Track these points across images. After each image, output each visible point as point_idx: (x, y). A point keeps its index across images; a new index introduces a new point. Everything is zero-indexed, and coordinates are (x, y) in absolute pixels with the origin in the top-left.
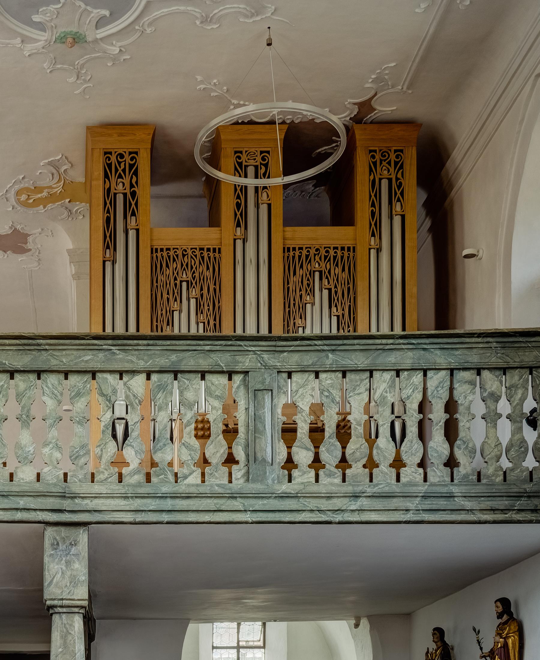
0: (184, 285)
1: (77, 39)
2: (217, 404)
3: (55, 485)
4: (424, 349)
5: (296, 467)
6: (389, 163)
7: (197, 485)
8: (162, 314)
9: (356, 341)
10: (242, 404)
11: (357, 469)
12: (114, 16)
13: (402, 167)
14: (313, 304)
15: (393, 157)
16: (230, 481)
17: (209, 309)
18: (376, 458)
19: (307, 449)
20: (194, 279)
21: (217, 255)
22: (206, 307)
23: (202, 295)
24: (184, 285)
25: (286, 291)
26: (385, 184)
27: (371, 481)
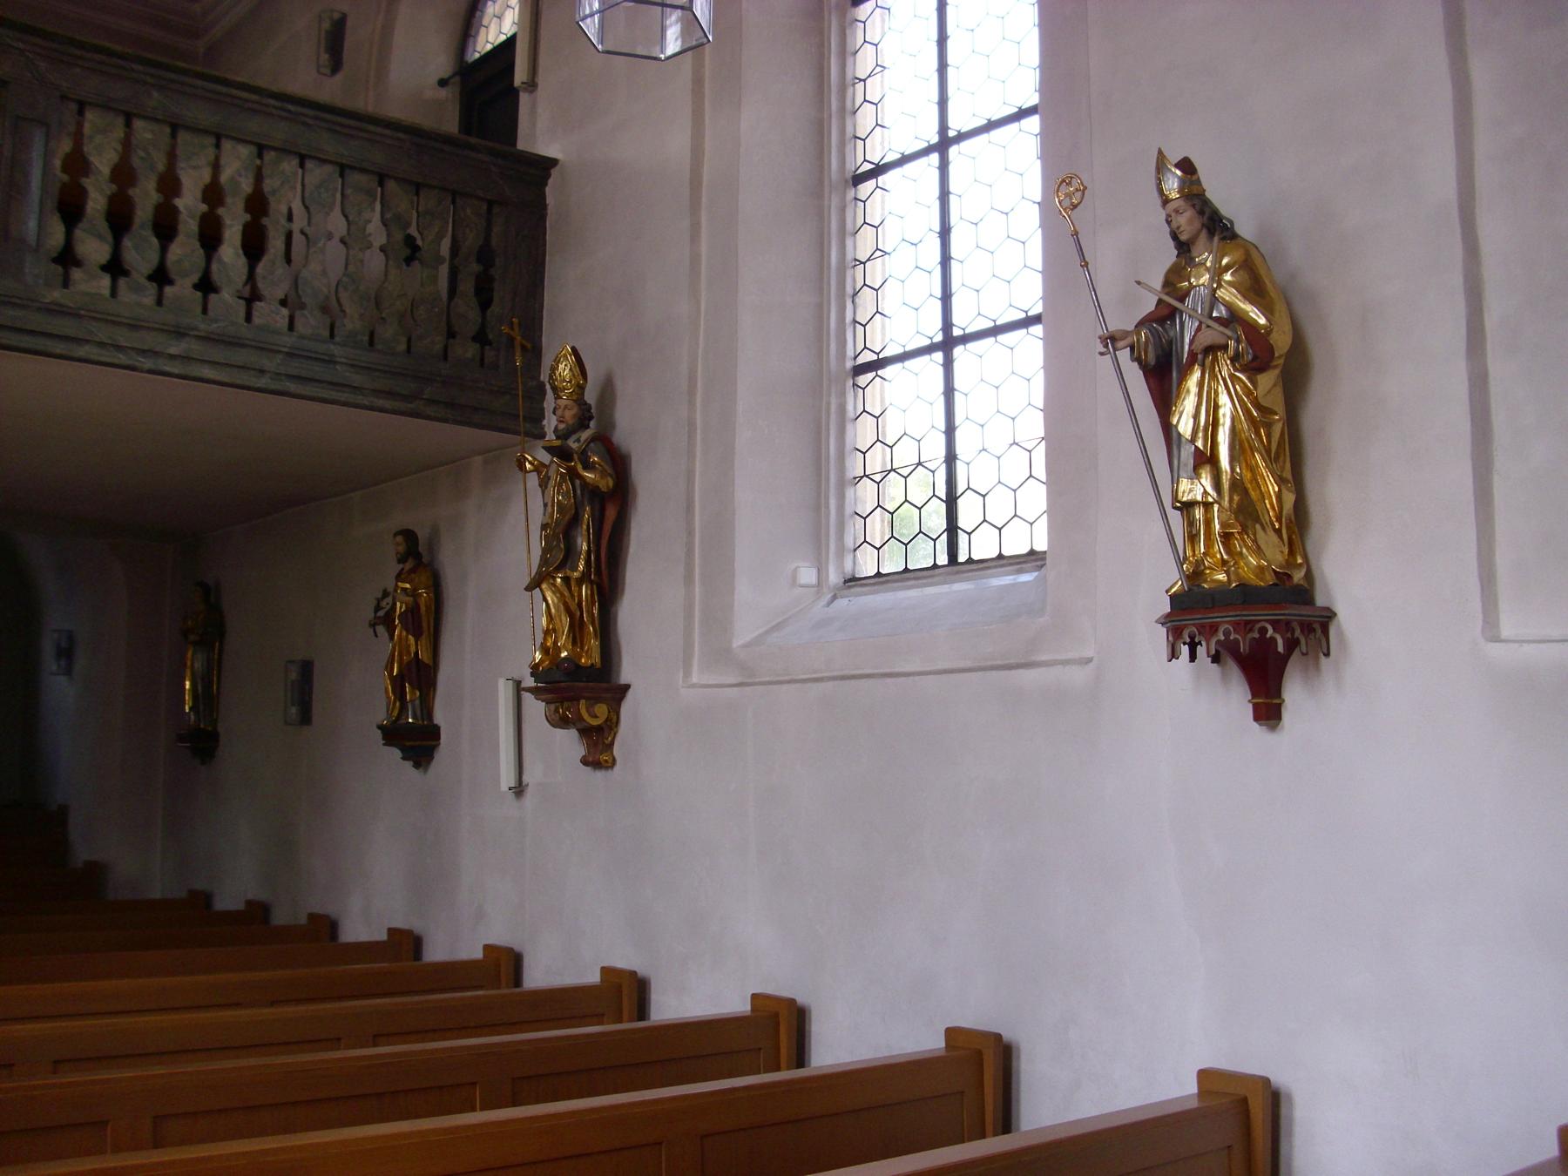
4: (304, 124)
5: (78, 263)
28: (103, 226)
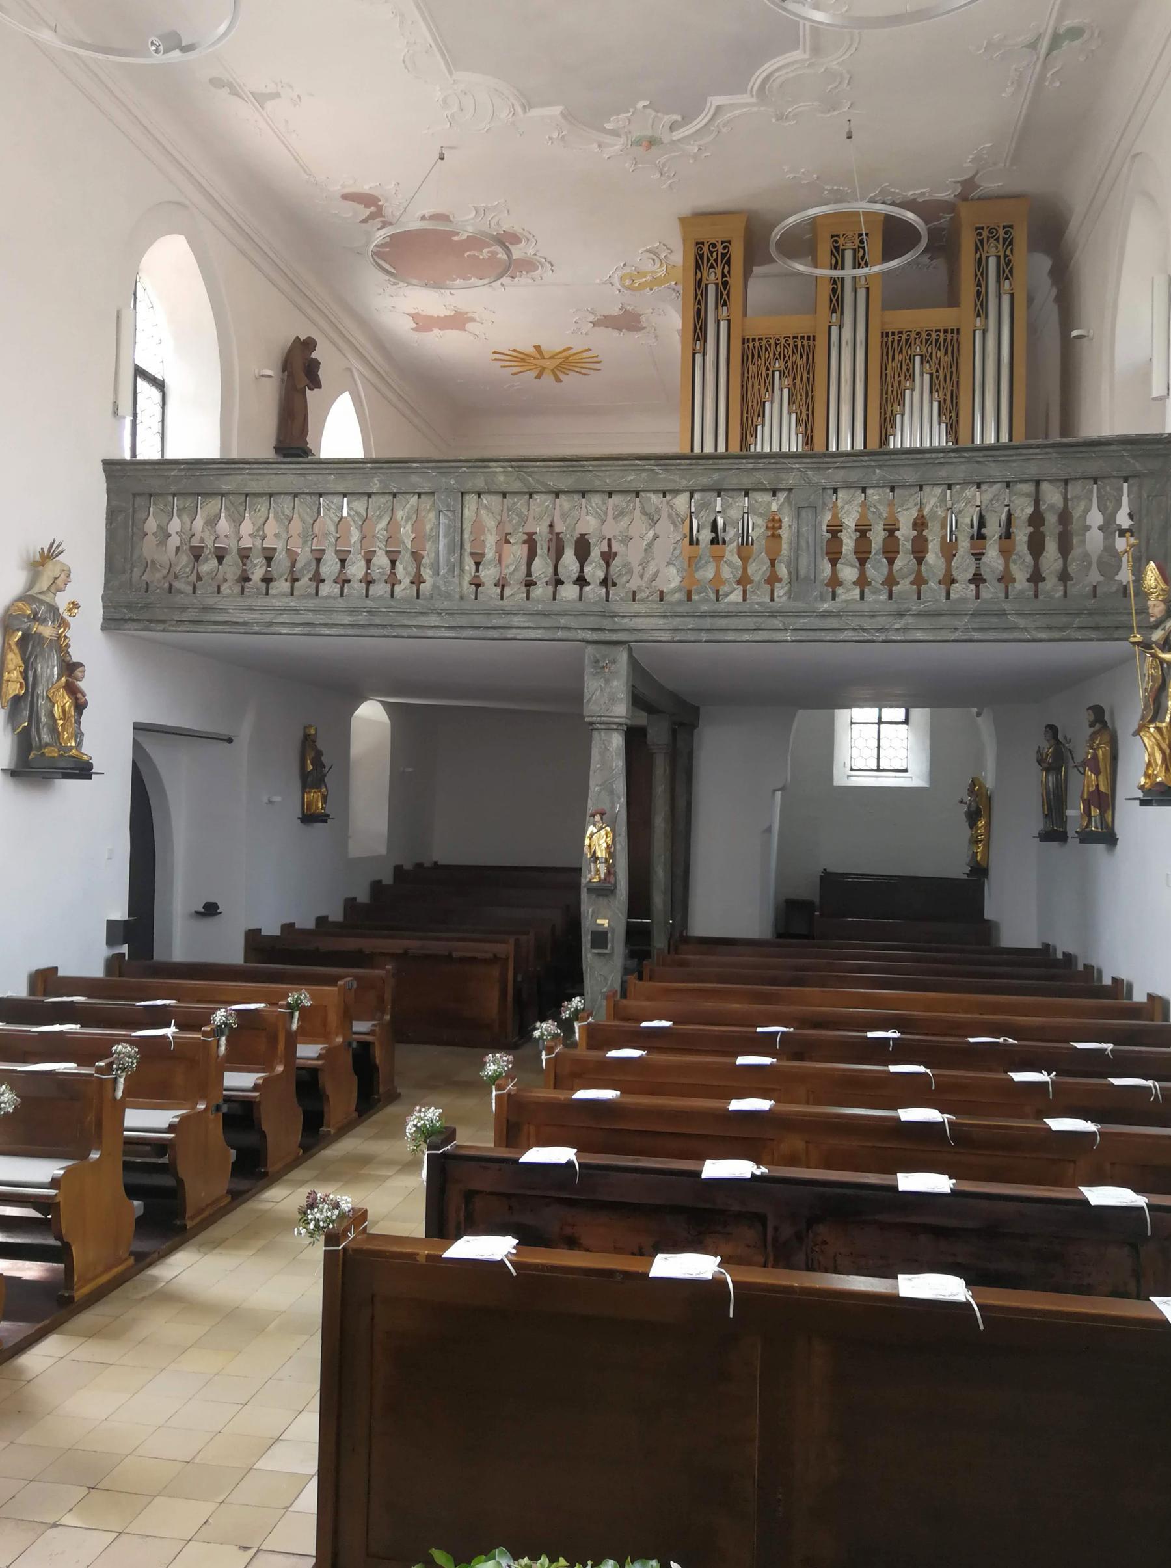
0: (777, 374)
1: (652, 142)
2: (760, 521)
3: (595, 603)
4: (978, 462)
6: (997, 240)
7: (737, 603)
9: (904, 456)
10: (786, 521)
11: (904, 586)
12: (687, 119)
13: (1011, 243)
14: (913, 390)
15: (1001, 233)
16: (772, 599)
18: (924, 574)
19: (853, 566)
21: (811, 343)
23: (794, 385)
24: (777, 374)
25: (883, 376)
26: (992, 262)
27: (919, 598)
28: (853, 558)
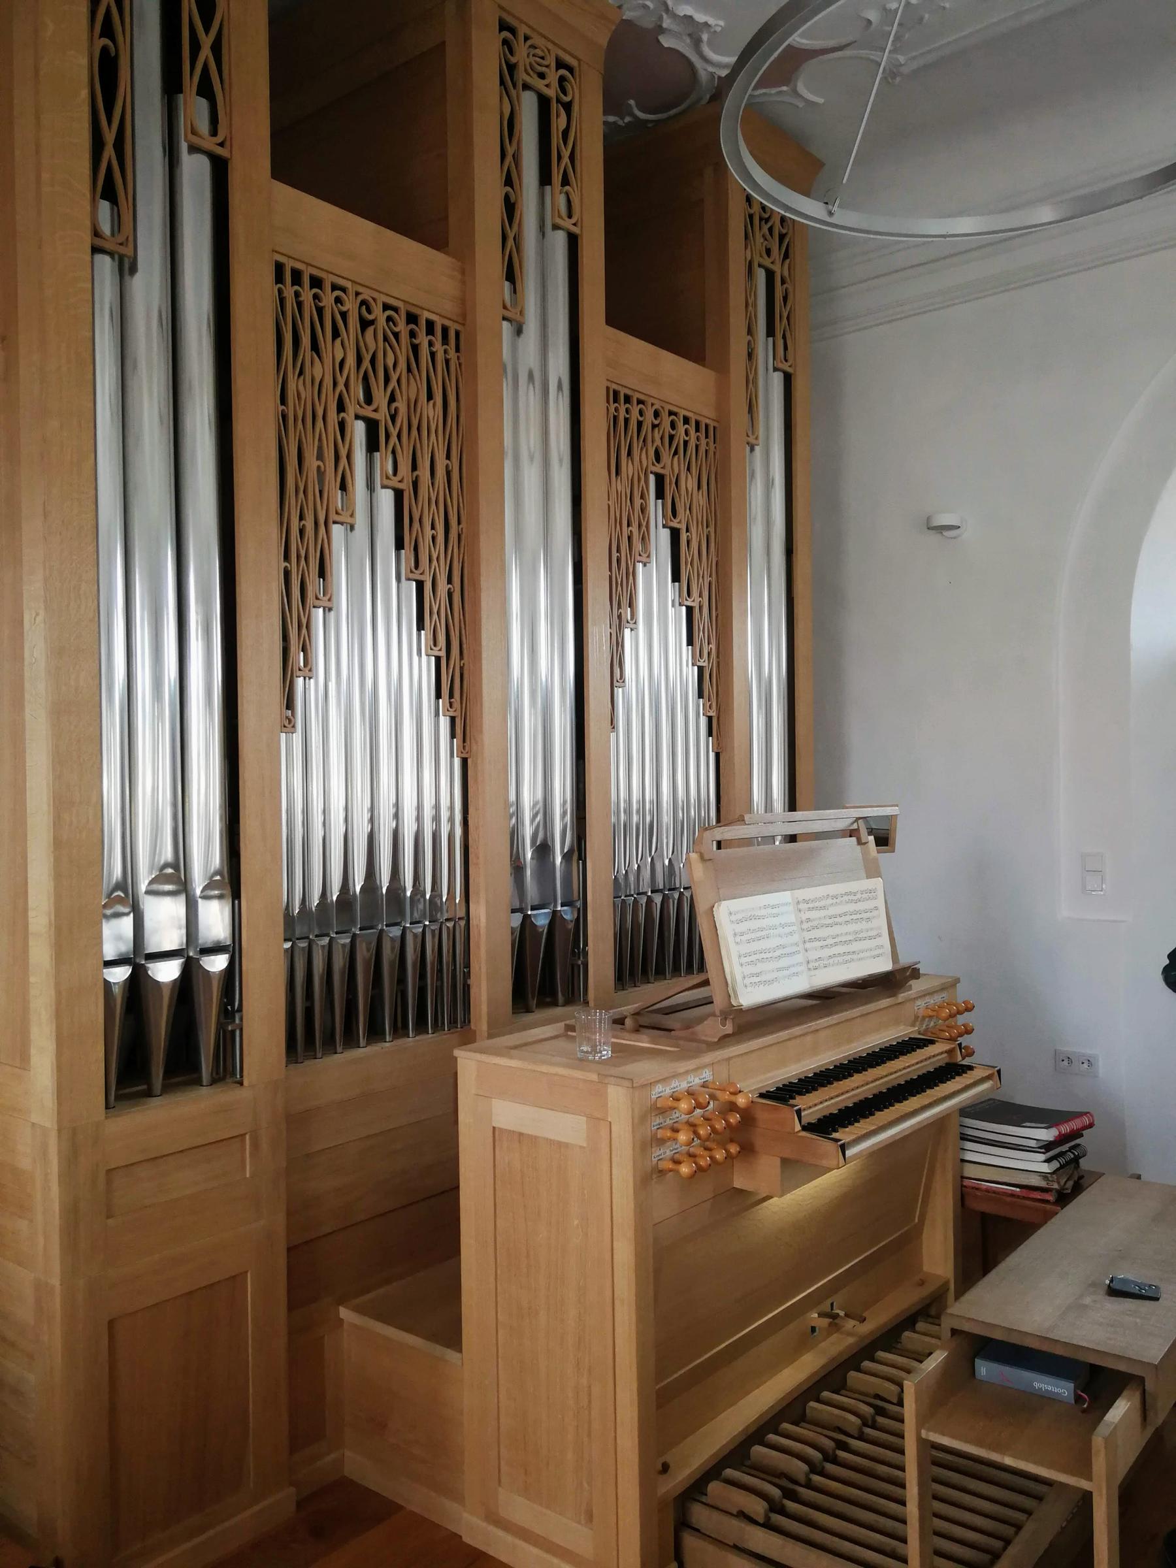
8: (302, 531)
17: (434, 538)
20: (393, 418)
22: (429, 533)
